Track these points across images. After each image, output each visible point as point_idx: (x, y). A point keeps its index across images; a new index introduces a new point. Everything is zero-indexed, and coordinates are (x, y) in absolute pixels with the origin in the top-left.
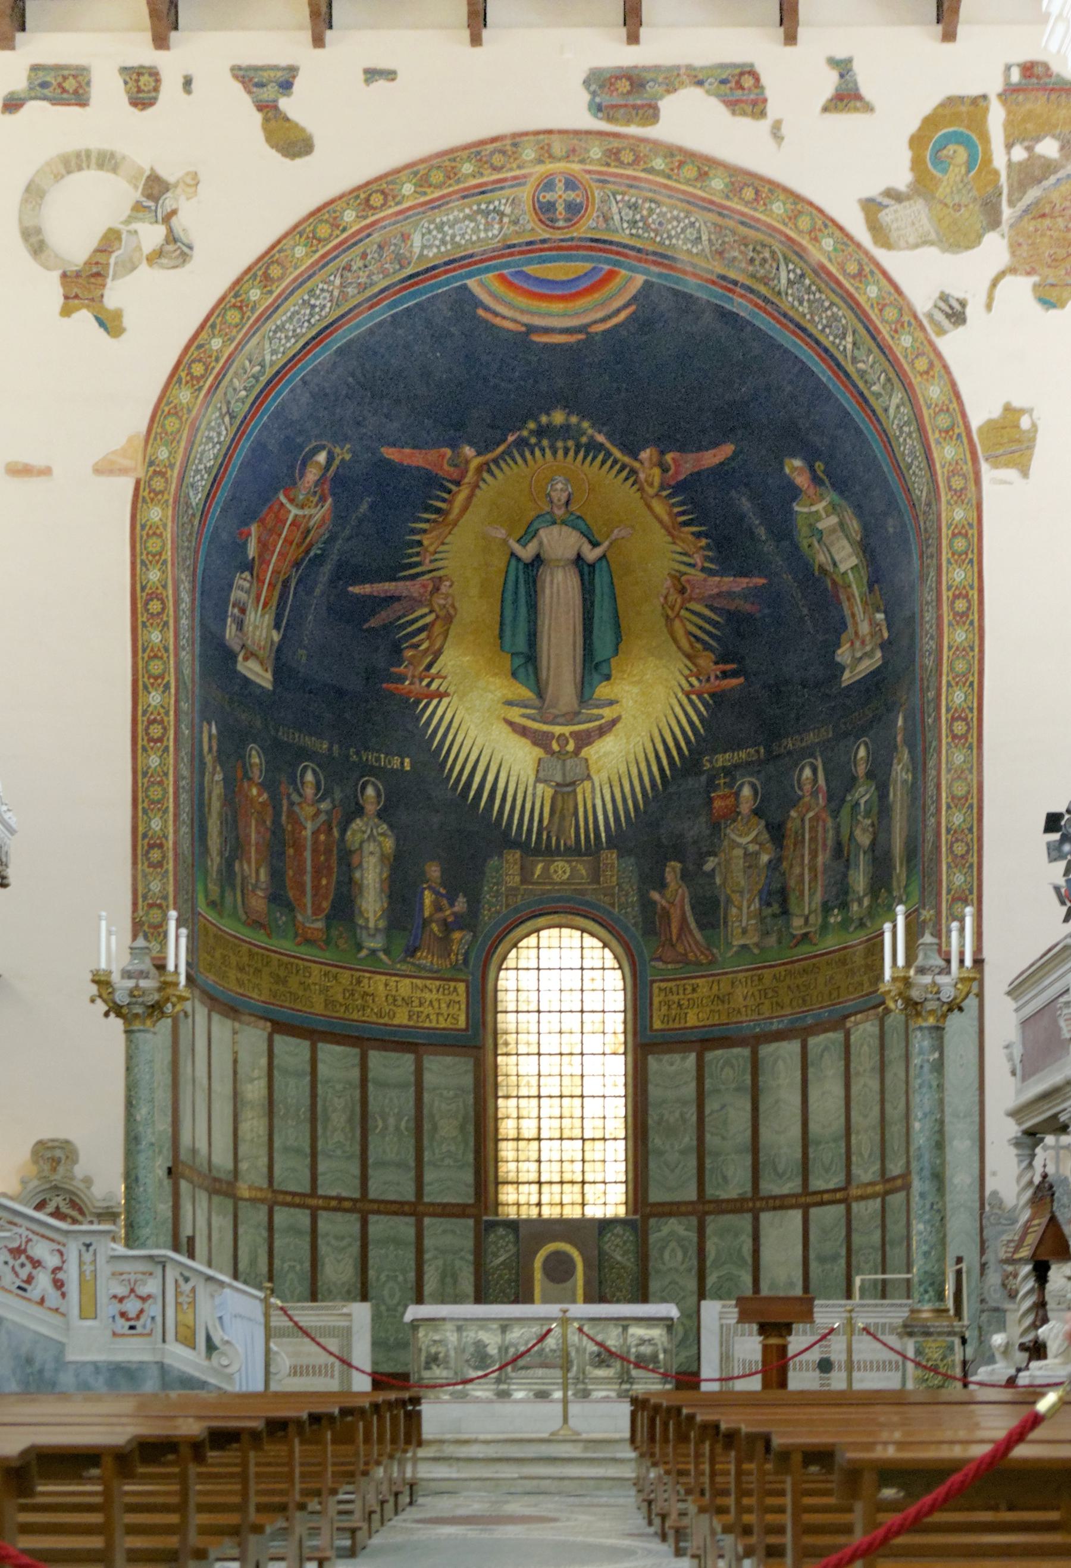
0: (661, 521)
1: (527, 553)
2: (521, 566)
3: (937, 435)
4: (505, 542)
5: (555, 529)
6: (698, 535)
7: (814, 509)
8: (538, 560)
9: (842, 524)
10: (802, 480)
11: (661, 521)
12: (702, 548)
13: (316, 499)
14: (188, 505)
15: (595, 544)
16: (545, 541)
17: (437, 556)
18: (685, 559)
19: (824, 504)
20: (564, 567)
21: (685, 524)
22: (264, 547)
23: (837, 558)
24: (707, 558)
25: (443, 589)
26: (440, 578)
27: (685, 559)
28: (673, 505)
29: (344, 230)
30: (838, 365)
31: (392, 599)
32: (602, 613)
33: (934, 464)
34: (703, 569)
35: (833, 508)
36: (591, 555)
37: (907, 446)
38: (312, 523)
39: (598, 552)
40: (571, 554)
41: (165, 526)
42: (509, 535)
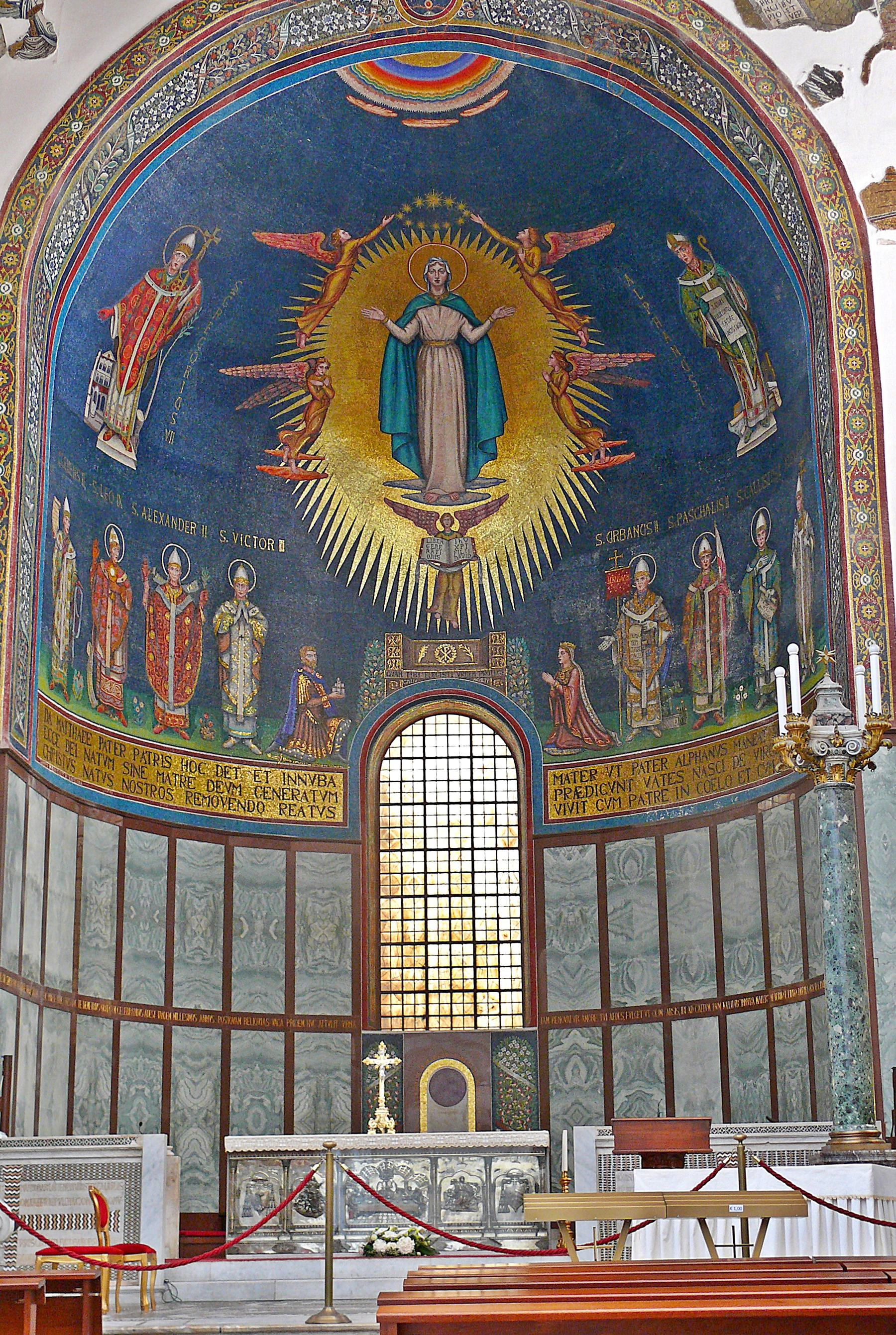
0: (542, 300)
1: (406, 334)
2: (400, 347)
3: (819, 199)
4: (382, 323)
5: (435, 310)
6: (581, 313)
7: (698, 282)
8: (418, 341)
9: (727, 295)
10: (685, 255)
11: (542, 300)
12: (585, 325)
13: (184, 282)
14: (42, 280)
15: (475, 325)
16: (424, 322)
17: (312, 338)
18: (570, 336)
19: (709, 276)
20: (444, 347)
21: (568, 301)
22: (128, 327)
23: (725, 329)
24: (592, 336)
25: (320, 371)
26: (316, 360)
27: (570, 336)
28: (555, 284)
29: (210, 20)
30: (715, 139)
31: (262, 382)
32: (486, 395)
33: (817, 226)
34: (588, 346)
35: (718, 281)
36: (473, 334)
37: (788, 212)
38: (180, 305)
39: (479, 331)
40: (451, 334)
41: (15, 300)
42: (388, 316)
